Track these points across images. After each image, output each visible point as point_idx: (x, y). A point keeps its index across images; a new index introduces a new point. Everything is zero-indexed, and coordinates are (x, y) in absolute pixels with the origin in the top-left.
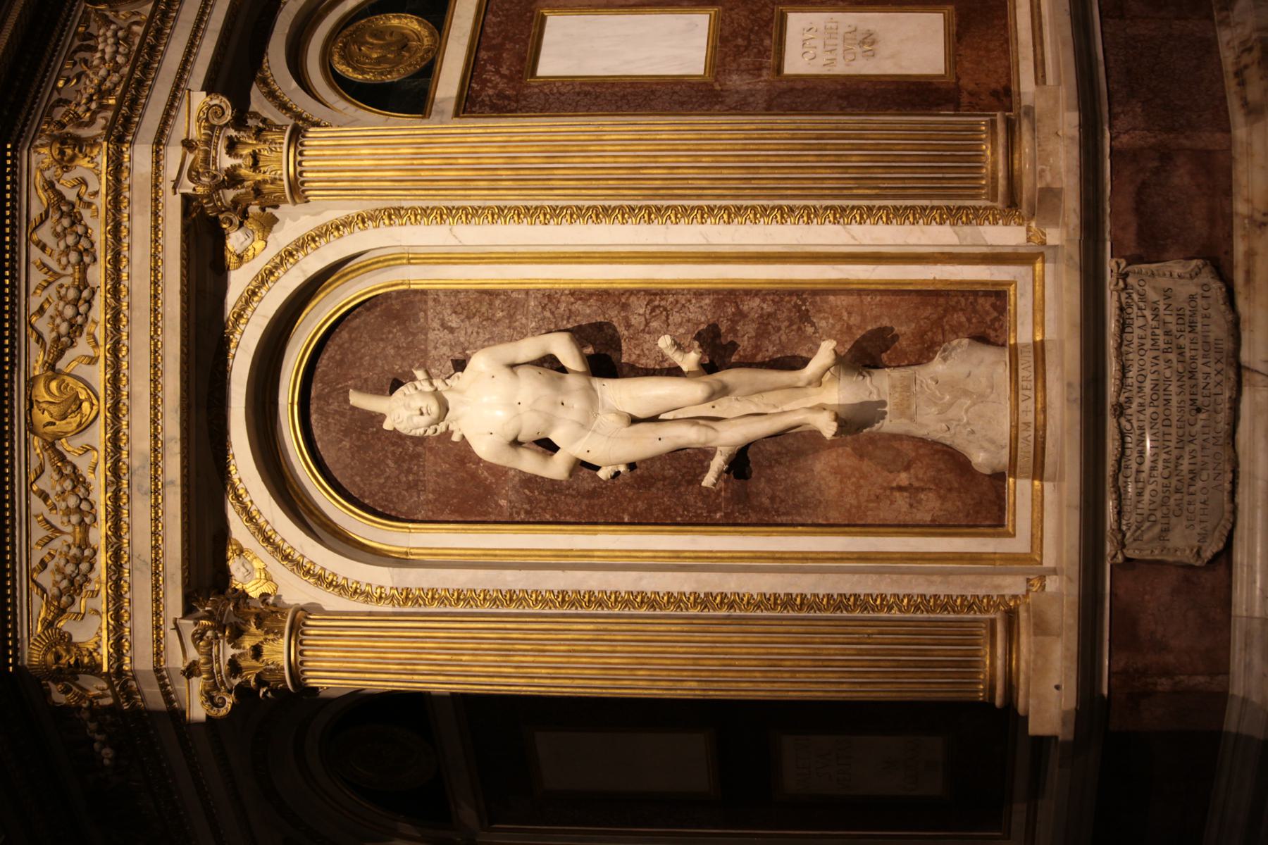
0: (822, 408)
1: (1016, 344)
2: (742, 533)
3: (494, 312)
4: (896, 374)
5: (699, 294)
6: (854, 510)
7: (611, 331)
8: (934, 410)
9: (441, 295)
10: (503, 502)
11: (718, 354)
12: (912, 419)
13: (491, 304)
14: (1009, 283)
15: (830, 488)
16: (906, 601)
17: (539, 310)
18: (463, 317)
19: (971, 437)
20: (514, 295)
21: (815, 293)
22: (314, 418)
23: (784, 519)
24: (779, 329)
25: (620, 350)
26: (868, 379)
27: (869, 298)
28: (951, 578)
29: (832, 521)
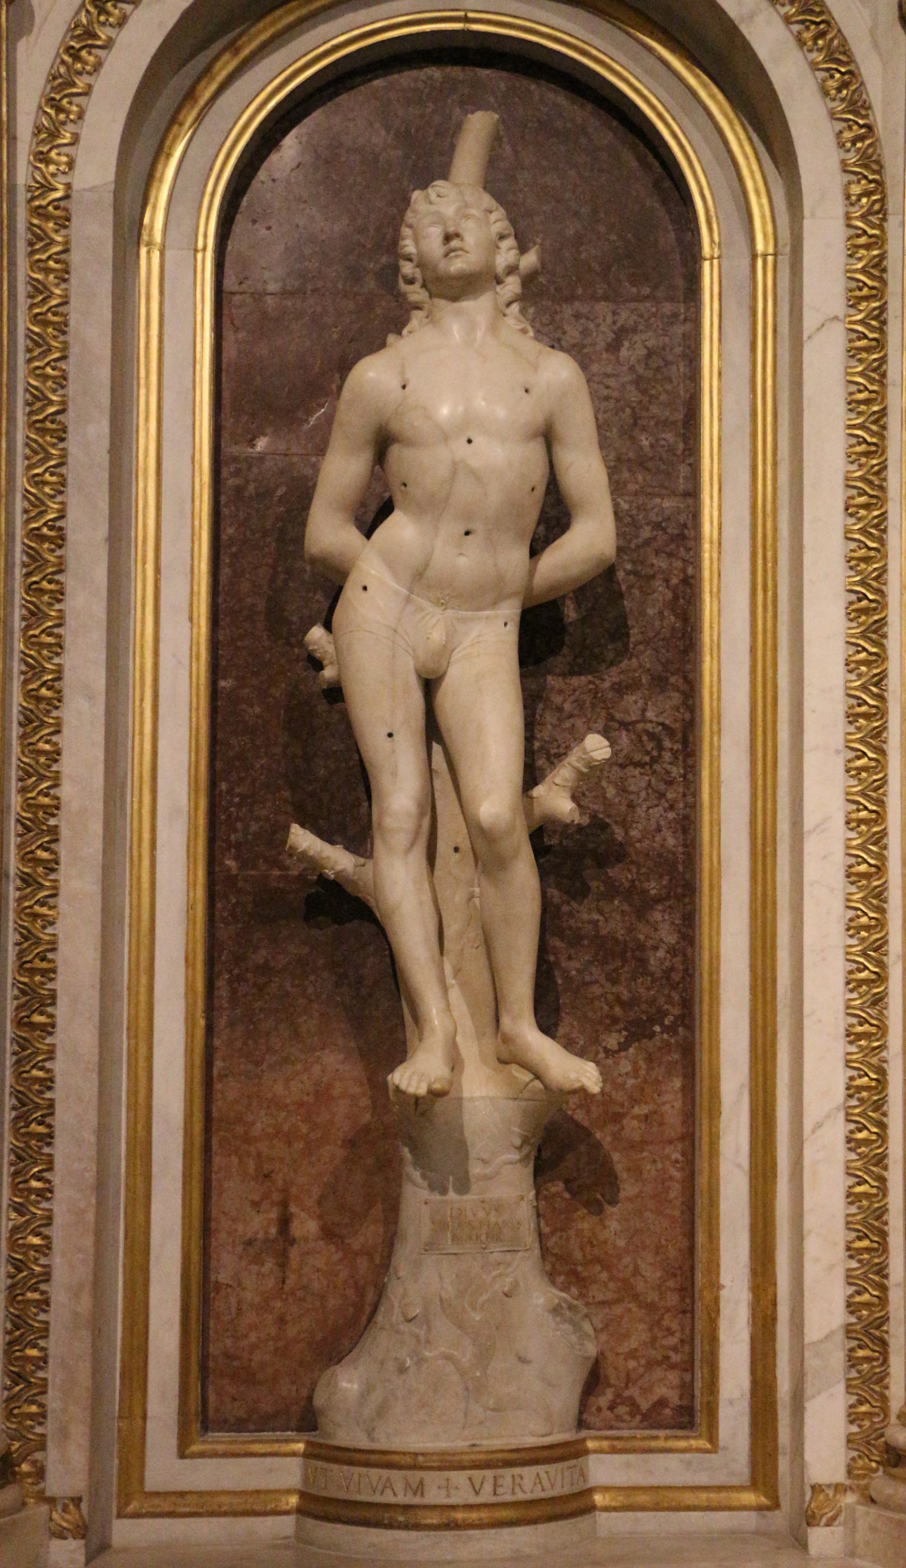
0: (455, 1063)
1: (587, 1452)
2: (191, 907)
3: (654, 435)
4: (525, 1213)
5: (687, 825)
6: (240, 1130)
7: (611, 655)
8: (450, 1291)
9: (688, 327)
10: (261, 444)
11: (567, 857)
12: (430, 1247)
13: (666, 424)
14: (712, 1438)
15: (287, 1081)
16: (36, 1241)
17: (653, 517)
18: (640, 369)
19: (391, 1366)
20: (684, 470)
21: (688, 1051)
22: (435, 73)
23: (223, 990)
24: (614, 982)
25: (572, 673)
26: (516, 1156)
27: (676, 1156)
28: (85, 1334)
29: (218, 1086)
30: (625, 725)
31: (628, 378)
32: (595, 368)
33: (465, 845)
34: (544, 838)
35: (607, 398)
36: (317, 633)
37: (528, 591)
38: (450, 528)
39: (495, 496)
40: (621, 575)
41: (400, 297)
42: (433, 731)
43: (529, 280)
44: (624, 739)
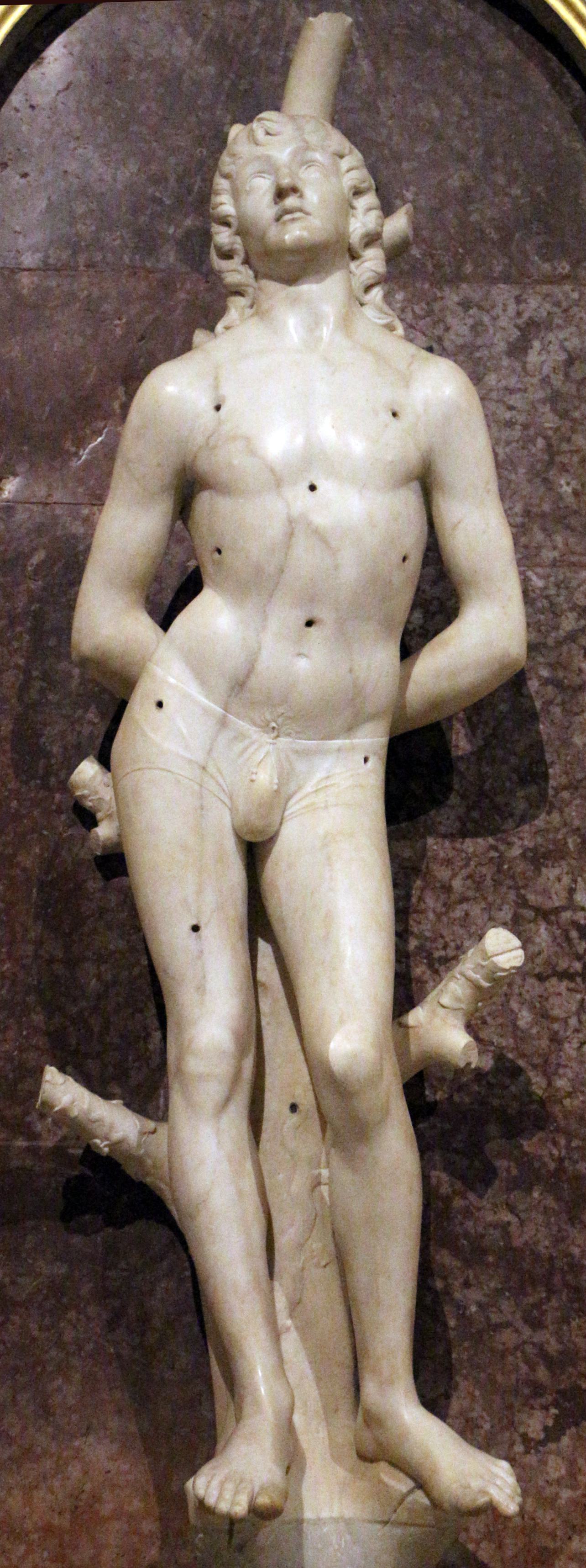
7: (520, 806)
18: (557, 381)
25: (464, 834)
30: (545, 914)
31: (540, 395)
32: (492, 379)
33: (307, 1100)
34: (425, 1089)
35: (510, 424)
36: (88, 771)
37: (399, 707)
38: (284, 616)
39: (350, 570)
40: (533, 685)
41: (213, 277)
42: (259, 921)
43: (396, 254)
44: (543, 934)
